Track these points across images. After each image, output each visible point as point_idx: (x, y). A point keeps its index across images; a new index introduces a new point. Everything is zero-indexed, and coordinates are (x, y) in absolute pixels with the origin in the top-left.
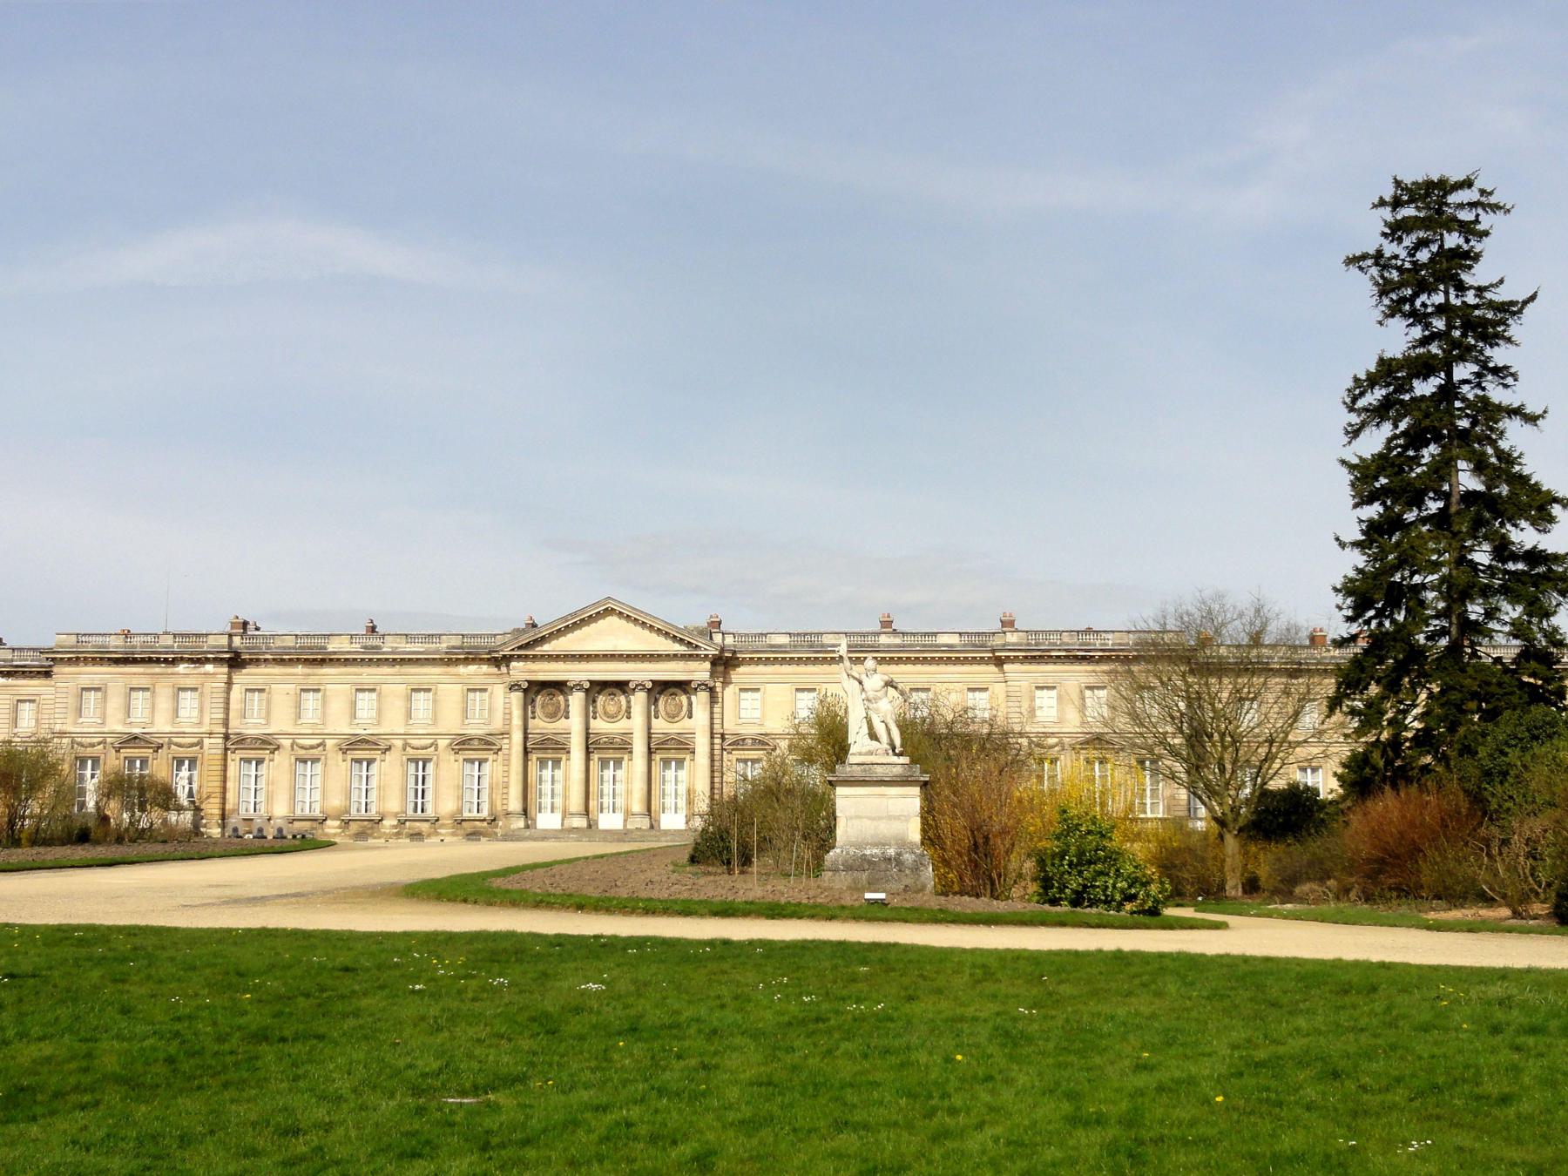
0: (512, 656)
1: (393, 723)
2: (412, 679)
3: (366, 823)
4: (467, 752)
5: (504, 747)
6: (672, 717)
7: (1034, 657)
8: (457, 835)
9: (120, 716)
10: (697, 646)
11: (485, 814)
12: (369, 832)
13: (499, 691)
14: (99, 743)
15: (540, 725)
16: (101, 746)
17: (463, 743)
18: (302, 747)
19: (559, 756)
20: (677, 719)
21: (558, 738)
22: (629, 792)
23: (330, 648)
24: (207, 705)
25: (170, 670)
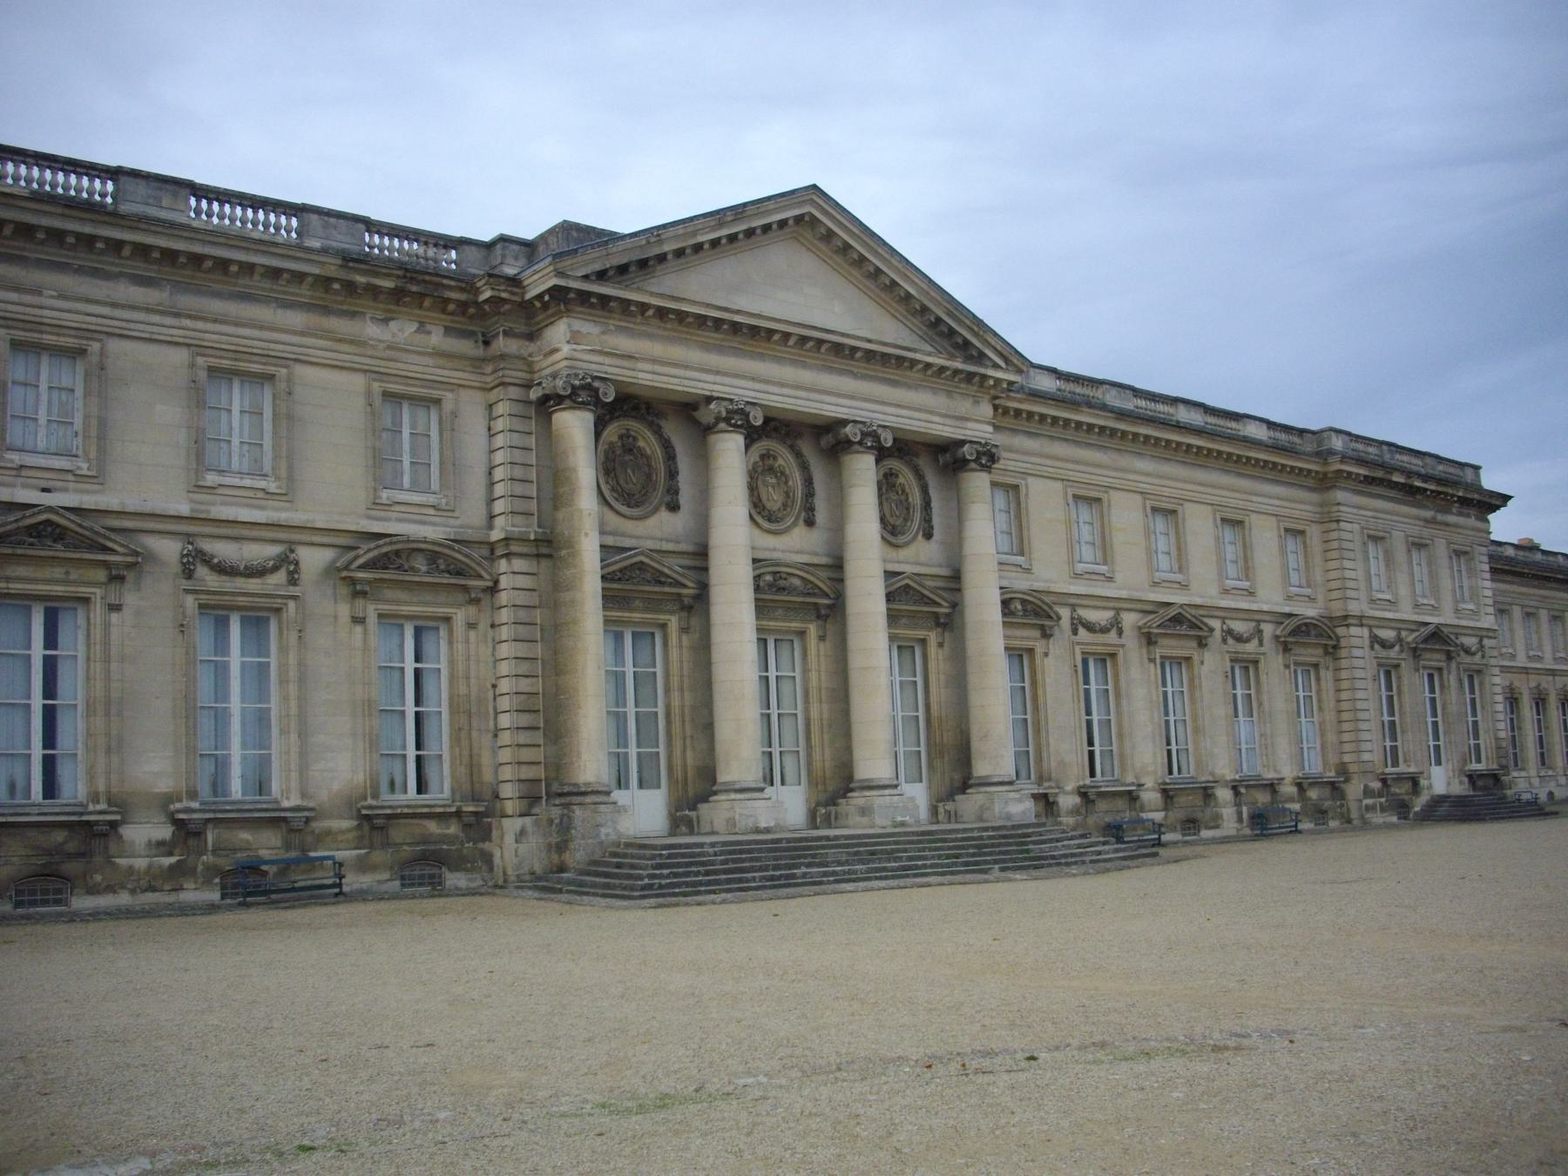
0: (584, 297)
2: (214, 334)
3: (59, 836)
4: (389, 594)
5: (504, 582)
8: (374, 868)
10: (982, 355)
11: (441, 792)
12: (71, 867)
19: (662, 617)
20: (901, 539)
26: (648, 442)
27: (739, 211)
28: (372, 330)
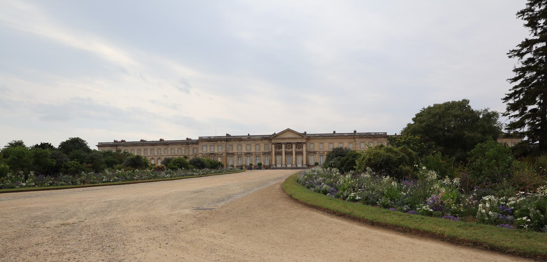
1: (253, 150)
2: (256, 143)
6: (299, 148)
7: (361, 137)
13: (270, 145)
15: (278, 150)
17: (265, 153)
18: (238, 155)
21: (280, 152)
22: (292, 161)
23: (242, 138)
24: (223, 148)
26: (280, 145)
27: (282, 131)
28: (264, 141)
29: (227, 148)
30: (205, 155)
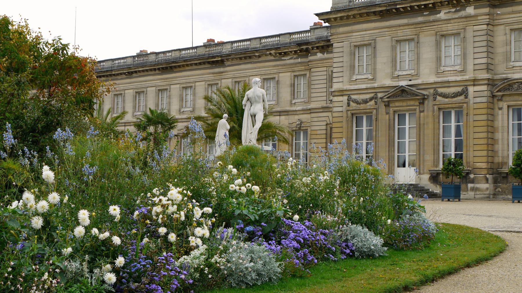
9: (388, 70)
14: (371, 99)
16: (372, 102)
24: (470, 50)
25: (432, 18)
29: (500, 50)
30: (365, 102)
